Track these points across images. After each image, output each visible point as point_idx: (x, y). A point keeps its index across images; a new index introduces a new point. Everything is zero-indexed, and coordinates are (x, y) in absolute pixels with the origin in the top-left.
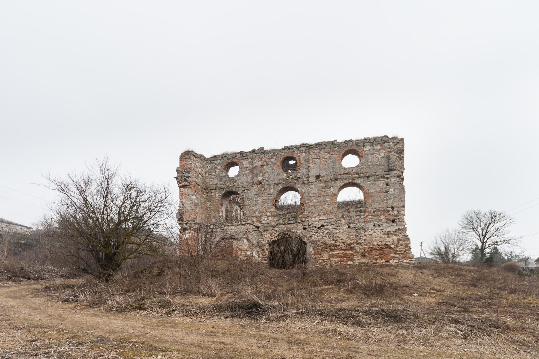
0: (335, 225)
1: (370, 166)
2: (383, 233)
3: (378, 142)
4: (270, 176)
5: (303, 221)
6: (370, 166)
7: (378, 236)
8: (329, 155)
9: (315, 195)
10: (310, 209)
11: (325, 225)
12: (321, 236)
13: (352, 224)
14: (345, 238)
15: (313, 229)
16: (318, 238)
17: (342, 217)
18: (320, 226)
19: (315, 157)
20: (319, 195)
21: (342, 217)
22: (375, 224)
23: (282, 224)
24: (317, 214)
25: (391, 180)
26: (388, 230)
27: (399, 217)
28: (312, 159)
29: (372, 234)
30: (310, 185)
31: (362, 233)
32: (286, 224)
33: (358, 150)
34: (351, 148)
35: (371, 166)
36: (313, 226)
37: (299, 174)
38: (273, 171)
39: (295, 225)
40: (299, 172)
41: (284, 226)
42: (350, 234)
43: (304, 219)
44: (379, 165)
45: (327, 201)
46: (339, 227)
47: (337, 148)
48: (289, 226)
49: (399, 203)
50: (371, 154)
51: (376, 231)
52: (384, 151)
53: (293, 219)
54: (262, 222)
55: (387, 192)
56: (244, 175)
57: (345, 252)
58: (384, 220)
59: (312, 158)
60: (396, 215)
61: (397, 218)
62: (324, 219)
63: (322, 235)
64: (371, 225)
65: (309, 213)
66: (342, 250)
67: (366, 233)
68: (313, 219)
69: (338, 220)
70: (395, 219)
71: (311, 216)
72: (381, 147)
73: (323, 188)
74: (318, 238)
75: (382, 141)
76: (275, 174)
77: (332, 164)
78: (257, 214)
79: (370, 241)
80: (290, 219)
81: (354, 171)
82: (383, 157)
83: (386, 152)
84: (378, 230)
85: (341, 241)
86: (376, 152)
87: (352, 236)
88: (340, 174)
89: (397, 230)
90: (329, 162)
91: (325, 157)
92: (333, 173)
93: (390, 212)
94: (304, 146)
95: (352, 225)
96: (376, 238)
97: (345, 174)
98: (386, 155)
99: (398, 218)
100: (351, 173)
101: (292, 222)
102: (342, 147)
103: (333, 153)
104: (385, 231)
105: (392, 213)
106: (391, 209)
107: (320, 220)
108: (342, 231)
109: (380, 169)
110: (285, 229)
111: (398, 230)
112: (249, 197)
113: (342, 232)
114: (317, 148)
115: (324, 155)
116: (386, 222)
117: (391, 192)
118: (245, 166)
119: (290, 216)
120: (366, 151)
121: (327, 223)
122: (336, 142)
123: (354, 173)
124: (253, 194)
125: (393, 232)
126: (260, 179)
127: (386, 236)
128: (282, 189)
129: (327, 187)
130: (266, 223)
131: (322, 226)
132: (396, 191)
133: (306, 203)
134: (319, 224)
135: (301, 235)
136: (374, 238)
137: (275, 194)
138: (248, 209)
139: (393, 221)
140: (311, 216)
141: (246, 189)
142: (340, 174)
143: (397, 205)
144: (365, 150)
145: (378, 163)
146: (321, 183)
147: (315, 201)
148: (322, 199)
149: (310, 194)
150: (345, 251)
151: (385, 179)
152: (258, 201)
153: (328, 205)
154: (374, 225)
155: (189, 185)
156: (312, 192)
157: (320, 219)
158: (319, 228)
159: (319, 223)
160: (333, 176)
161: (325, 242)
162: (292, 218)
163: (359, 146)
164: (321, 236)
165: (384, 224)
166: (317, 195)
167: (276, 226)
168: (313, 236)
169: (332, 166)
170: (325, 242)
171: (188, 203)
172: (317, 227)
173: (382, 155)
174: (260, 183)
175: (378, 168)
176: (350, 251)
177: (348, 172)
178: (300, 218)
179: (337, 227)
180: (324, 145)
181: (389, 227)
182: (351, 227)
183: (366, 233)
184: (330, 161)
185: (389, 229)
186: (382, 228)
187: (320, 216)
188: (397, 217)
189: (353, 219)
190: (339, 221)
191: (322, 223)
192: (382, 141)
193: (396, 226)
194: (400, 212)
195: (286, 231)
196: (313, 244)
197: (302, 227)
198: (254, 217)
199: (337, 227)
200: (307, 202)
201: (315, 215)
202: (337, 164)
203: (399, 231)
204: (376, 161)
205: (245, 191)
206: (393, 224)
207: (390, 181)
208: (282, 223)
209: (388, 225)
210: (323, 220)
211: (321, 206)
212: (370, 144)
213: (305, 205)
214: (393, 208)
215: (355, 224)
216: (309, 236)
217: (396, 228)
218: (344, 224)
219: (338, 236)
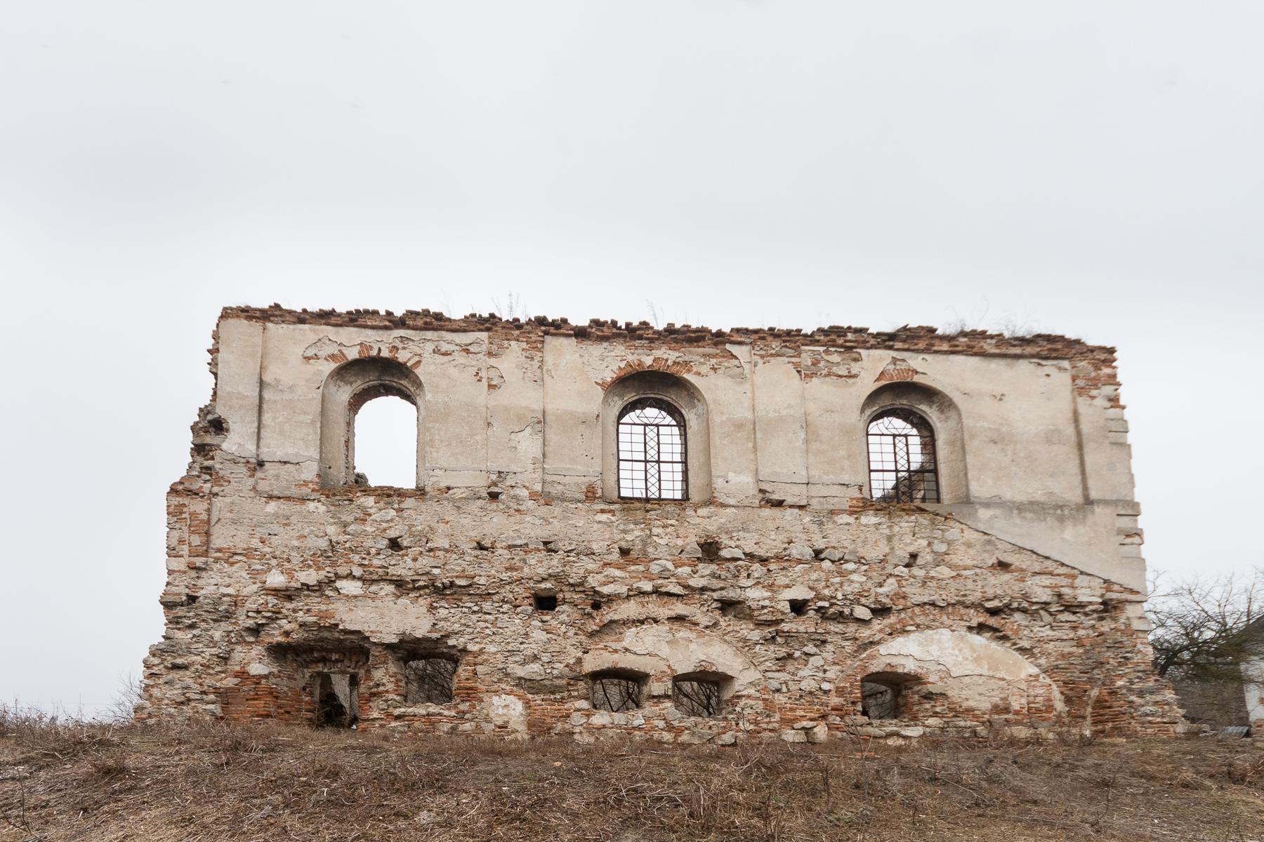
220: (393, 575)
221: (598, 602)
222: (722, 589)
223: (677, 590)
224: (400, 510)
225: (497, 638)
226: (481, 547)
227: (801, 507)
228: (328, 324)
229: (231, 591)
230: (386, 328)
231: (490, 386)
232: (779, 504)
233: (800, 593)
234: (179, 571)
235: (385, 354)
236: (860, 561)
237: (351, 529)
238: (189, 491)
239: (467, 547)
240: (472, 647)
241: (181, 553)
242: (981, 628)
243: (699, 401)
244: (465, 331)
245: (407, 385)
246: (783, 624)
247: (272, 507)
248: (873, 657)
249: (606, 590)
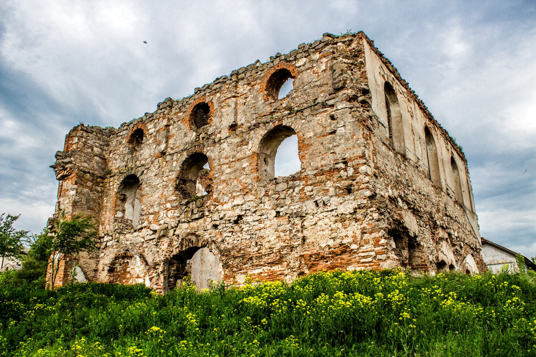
0: (257, 212)
1: (306, 90)
2: (333, 219)
3: (316, 48)
4: (175, 140)
5: (212, 213)
6: (306, 90)
7: (327, 226)
8: (249, 88)
9: (227, 161)
10: (220, 187)
11: (243, 215)
12: (238, 239)
13: (282, 207)
14: (273, 238)
15: (227, 225)
16: (235, 242)
17: (266, 195)
18: (236, 218)
19: (229, 96)
20: (234, 160)
21: (266, 195)
22: (318, 202)
23: (185, 222)
24: (230, 195)
25: (339, 108)
26: (341, 212)
27: (358, 180)
28: (225, 100)
29: (315, 224)
30: (222, 143)
31: (297, 225)
32: (189, 222)
33: (288, 69)
34: (279, 68)
35: (308, 91)
36: (226, 220)
37: (211, 129)
38: (180, 131)
39: (201, 221)
40: (211, 126)
41: (186, 225)
42: (280, 229)
43: (212, 207)
44: (321, 86)
45: (244, 168)
46: (263, 217)
47: (260, 72)
48: (194, 224)
49: (355, 150)
50: (308, 69)
51: (321, 216)
52: (325, 60)
53: (198, 211)
54: (160, 222)
55: (334, 132)
56: (148, 146)
57: (272, 269)
58: (332, 191)
59: (225, 98)
60: (352, 177)
61: (354, 183)
62: (240, 203)
63: (241, 235)
64: (310, 206)
65: (219, 195)
66: (268, 263)
67: (305, 223)
68: (225, 207)
69: (261, 203)
70: (351, 185)
71: (221, 201)
72: (320, 54)
73: (238, 146)
74: (235, 242)
75: (322, 45)
76: (181, 136)
77: (254, 101)
78: (156, 209)
79: (314, 240)
80: (195, 211)
81: (284, 105)
82: (324, 71)
83: (327, 61)
84: (325, 214)
85: (267, 245)
86: (314, 65)
87: (284, 231)
88: (265, 116)
89: (356, 209)
90: (248, 99)
91: (244, 92)
92: (255, 116)
93: (342, 171)
94: (218, 81)
95: (282, 209)
96: (324, 233)
97: (272, 113)
98: (329, 65)
99: (356, 181)
100: (279, 110)
101: (197, 216)
102: (266, 70)
103: (255, 82)
104: (336, 214)
105: (345, 174)
106: (343, 166)
107: (235, 206)
108: (268, 223)
109: (321, 92)
110: (189, 231)
111: (359, 208)
112: (148, 181)
113: (268, 226)
114: (231, 80)
115: (242, 90)
116: (336, 195)
117: (341, 131)
118: (150, 131)
119: (194, 206)
120: (299, 67)
121: (246, 210)
122: (258, 65)
123: (285, 108)
124: (153, 175)
125: (351, 214)
126: (162, 149)
127: (340, 225)
128: (186, 158)
129: (244, 142)
130: (164, 223)
131: (240, 217)
132: (349, 127)
133: (215, 178)
134: (233, 214)
135: (210, 240)
136: (321, 233)
137: (178, 169)
138: (145, 202)
139: (349, 190)
140: (221, 201)
141: (146, 169)
142: (265, 116)
143: (352, 156)
144: (297, 65)
145: (318, 83)
146: (236, 138)
147: (228, 171)
148: (238, 165)
149: (222, 160)
150: (271, 267)
151: (329, 109)
152: (158, 186)
153: (244, 176)
154: (317, 205)
155: (70, 175)
156: (224, 156)
157: (234, 204)
158: (236, 222)
159: (234, 213)
160: (254, 121)
161: (243, 250)
162: (197, 209)
163: (290, 61)
164: (238, 239)
165: (332, 199)
166: (231, 160)
167: (176, 227)
168: (227, 239)
169: (253, 104)
170: (243, 250)
171: (65, 202)
172: (230, 221)
173: (323, 67)
174: (163, 154)
175: (319, 91)
176: (280, 266)
177: (276, 109)
178: (207, 207)
179: (259, 218)
180: (242, 73)
181: (341, 204)
182: (281, 214)
183: (305, 223)
184: (251, 96)
185: (341, 210)
186: (330, 209)
187: (234, 198)
188: (354, 180)
189: (282, 196)
190: (262, 205)
191: (238, 212)
192: (322, 45)
193: (354, 199)
194: (358, 168)
195: (188, 234)
196: (223, 255)
197: (211, 224)
198: (151, 214)
199: (259, 218)
200: (216, 176)
201: (226, 198)
202: (260, 99)
203: (362, 211)
204: (315, 80)
205: (145, 172)
206: (348, 197)
207: (338, 110)
208: (183, 220)
209: (340, 200)
210: (238, 205)
211: (236, 178)
212: (305, 54)
213: (214, 181)
214: (345, 163)
215: (287, 207)
216: (220, 240)
217: (355, 205)
218: (269, 208)
219: (262, 235)
220: (409, 200)
221: (435, 226)
222: (448, 228)
223: (444, 226)
224: (406, 166)
225: (424, 240)
226: (420, 193)
227: (451, 198)
228: (381, 60)
229: (383, 194)
230: (391, 72)
231: (412, 116)
232: (448, 195)
233: (456, 235)
234: (370, 175)
235: (391, 83)
236: (459, 223)
237: (400, 170)
238: (368, 127)
239: (418, 191)
240: (422, 244)
241: (370, 164)
242: (472, 255)
243: (431, 144)
244: (403, 86)
245: (389, 99)
246: (456, 247)
247: (384, 148)
248: (465, 264)
249: (438, 222)
